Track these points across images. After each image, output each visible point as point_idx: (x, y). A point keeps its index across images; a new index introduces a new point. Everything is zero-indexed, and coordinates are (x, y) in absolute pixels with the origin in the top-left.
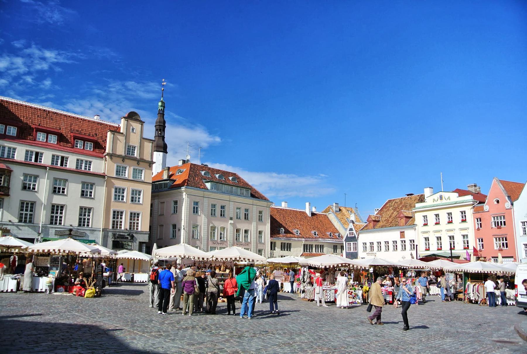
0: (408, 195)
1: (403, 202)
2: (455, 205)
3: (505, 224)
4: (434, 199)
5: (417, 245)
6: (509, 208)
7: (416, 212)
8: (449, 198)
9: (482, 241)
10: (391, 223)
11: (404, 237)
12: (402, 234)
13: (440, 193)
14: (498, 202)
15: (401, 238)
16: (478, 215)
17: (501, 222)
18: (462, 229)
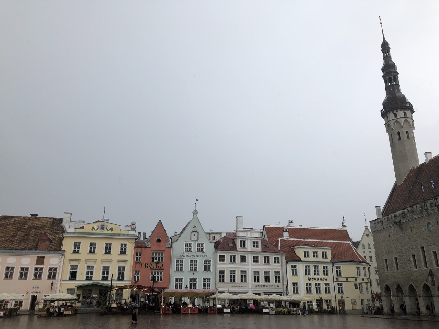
0: (32, 215)
1: (29, 222)
2: (118, 237)
3: (162, 261)
4: (93, 228)
5: (113, 275)
7: (66, 236)
9: (138, 274)
10: (19, 244)
11: (43, 264)
12: (40, 260)
13: (103, 223)
14: (159, 241)
15: (37, 264)
16: (139, 250)
17: (159, 258)
18: (119, 261)
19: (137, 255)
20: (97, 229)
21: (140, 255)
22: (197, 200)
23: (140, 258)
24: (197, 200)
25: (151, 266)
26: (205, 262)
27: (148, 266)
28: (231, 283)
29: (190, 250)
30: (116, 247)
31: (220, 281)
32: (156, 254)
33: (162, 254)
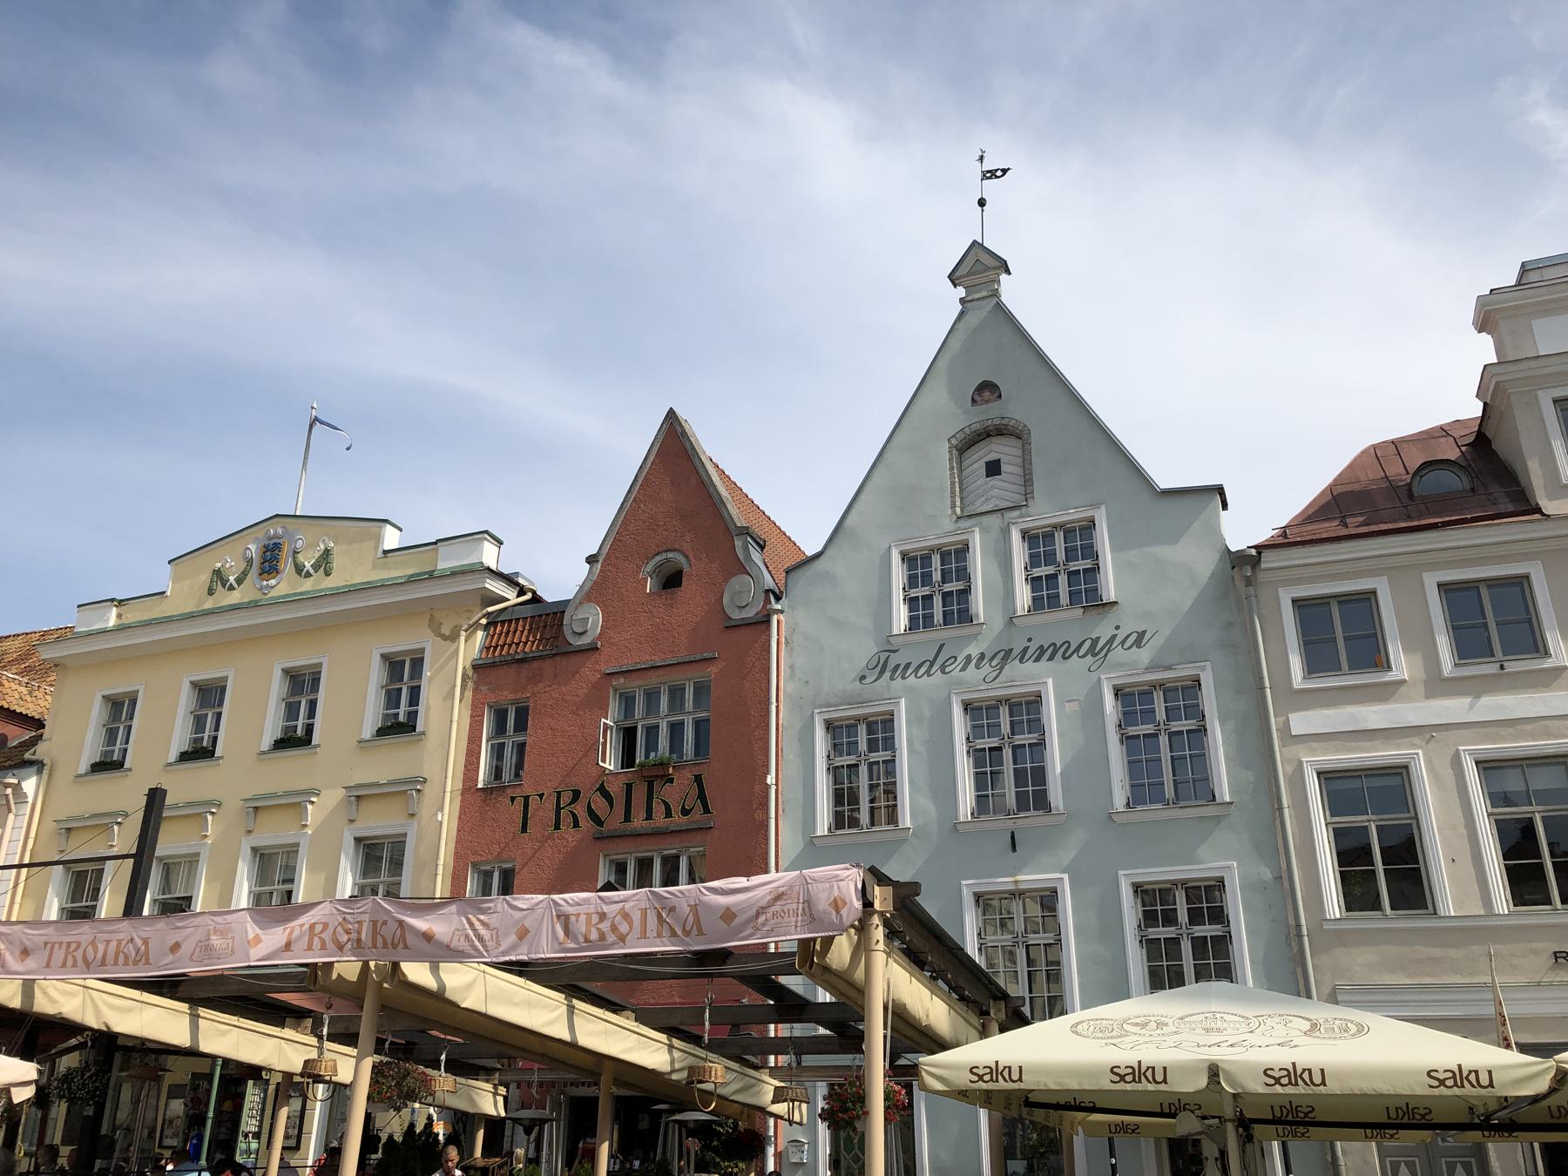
6: (750, 613)
8: (324, 562)
14: (672, 580)
17: (676, 729)
19: (500, 728)
20: (239, 581)
21: (521, 726)
22: (991, 175)
23: (521, 748)
24: (991, 175)
25: (600, 804)
26: (1132, 699)
27: (580, 810)
28: (1537, 915)
29: (959, 611)
30: (351, 699)
31: (1358, 894)
32: (652, 697)
33: (701, 690)
